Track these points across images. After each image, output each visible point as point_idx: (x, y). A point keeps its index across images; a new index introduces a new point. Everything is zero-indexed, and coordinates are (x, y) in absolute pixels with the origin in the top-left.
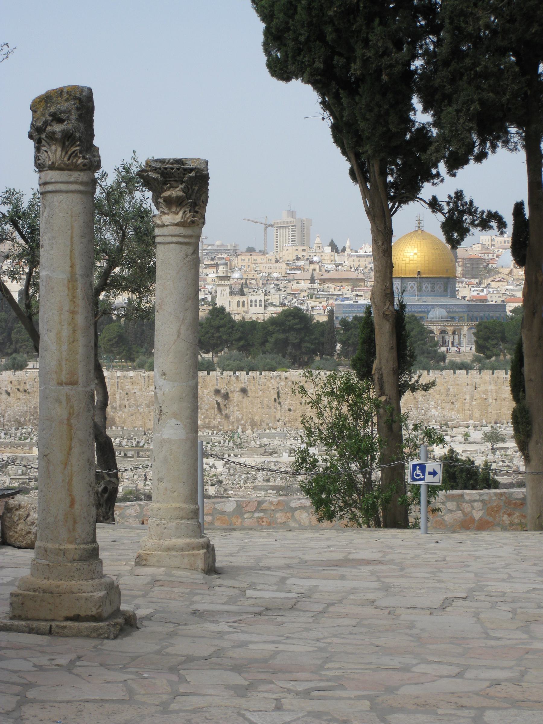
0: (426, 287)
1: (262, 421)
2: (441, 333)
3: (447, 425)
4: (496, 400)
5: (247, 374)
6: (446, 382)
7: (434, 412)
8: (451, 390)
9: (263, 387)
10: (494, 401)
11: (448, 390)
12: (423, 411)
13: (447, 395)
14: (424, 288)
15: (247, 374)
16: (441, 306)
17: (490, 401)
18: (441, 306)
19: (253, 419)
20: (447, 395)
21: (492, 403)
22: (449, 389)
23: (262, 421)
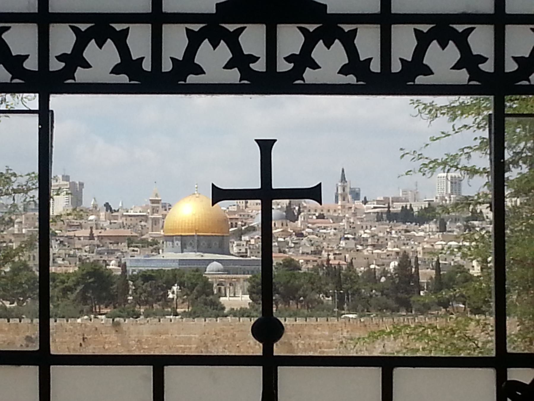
0: (204, 244)
2: (218, 285)
8: (237, 336)
11: (234, 336)
14: (201, 244)
16: (217, 261)
18: (217, 261)
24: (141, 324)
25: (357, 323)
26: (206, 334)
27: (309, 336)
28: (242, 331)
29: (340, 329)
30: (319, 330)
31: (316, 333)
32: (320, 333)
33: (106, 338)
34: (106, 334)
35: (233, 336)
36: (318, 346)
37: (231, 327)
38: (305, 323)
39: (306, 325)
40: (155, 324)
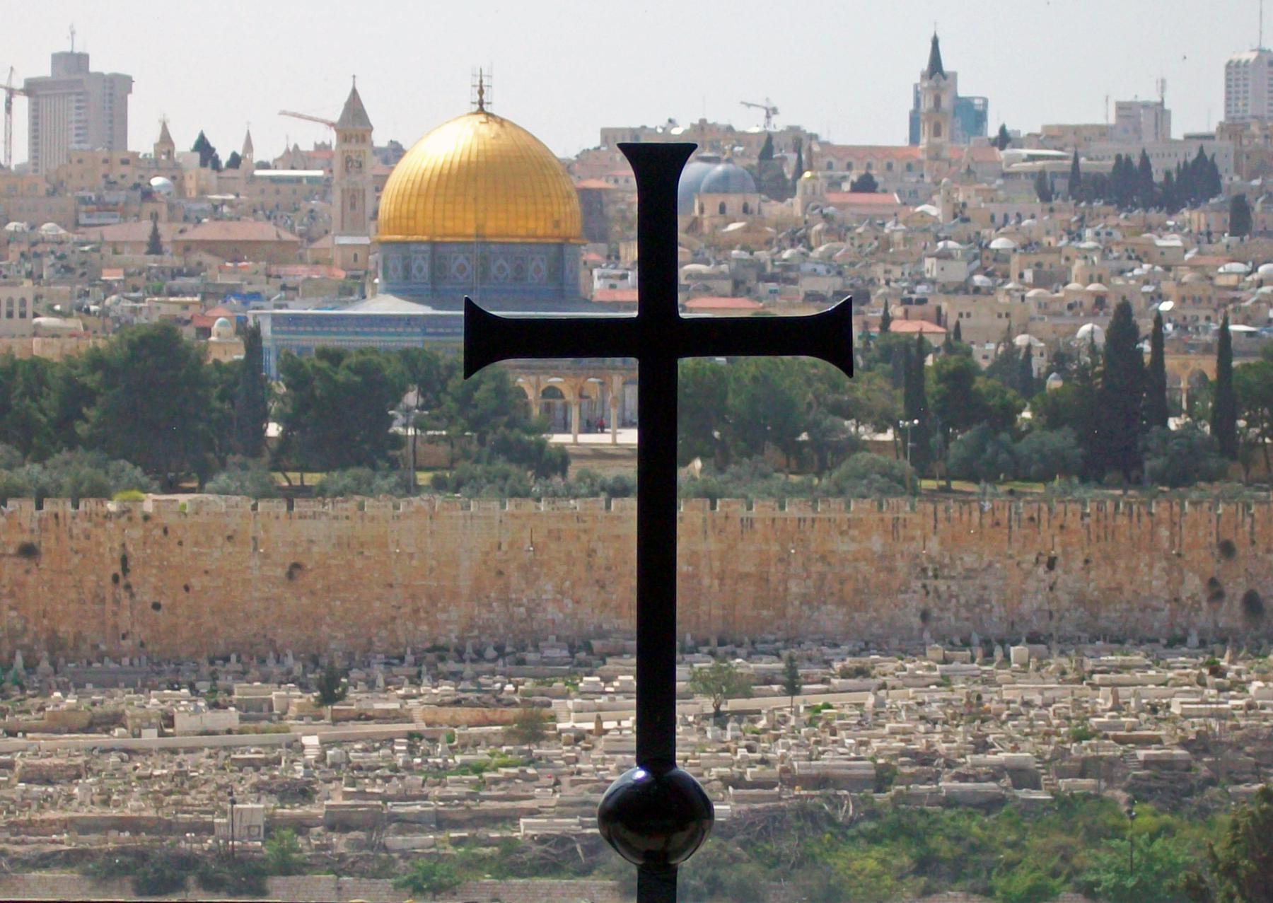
0: (501, 268)
1: (79, 637)
3: (589, 649)
4: (722, 580)
5: (39, 506)
6: (585, 531)
7: (552, 612)
8: (600, 553)
9: (84, 543)
10: (716, 582)
11: (591, 553)
12: (522, 610)
13: (590, 567)
14: (494, 270)
15: (39, 506)
17: (706, 581)
19: (54, 632)
20: (590, 567)
21: (710, 587)
22: (594, 551)
23: (79, 637)
24: (302, 517)
25: (970, 514)
26: (504, 547)
27: (823, 558)
28: (618, 537)
29: (918, 533)
30: (853, 539)
31: (844, 546)
32: (853, 547)
33: (194, 556)
34: (196, 544)
35: (589, 556)
36: (849, 588)
37: (582, 525)
38: (812, 515)
39: (813, 520)
40: (347, 518)
